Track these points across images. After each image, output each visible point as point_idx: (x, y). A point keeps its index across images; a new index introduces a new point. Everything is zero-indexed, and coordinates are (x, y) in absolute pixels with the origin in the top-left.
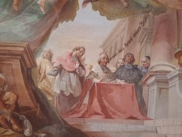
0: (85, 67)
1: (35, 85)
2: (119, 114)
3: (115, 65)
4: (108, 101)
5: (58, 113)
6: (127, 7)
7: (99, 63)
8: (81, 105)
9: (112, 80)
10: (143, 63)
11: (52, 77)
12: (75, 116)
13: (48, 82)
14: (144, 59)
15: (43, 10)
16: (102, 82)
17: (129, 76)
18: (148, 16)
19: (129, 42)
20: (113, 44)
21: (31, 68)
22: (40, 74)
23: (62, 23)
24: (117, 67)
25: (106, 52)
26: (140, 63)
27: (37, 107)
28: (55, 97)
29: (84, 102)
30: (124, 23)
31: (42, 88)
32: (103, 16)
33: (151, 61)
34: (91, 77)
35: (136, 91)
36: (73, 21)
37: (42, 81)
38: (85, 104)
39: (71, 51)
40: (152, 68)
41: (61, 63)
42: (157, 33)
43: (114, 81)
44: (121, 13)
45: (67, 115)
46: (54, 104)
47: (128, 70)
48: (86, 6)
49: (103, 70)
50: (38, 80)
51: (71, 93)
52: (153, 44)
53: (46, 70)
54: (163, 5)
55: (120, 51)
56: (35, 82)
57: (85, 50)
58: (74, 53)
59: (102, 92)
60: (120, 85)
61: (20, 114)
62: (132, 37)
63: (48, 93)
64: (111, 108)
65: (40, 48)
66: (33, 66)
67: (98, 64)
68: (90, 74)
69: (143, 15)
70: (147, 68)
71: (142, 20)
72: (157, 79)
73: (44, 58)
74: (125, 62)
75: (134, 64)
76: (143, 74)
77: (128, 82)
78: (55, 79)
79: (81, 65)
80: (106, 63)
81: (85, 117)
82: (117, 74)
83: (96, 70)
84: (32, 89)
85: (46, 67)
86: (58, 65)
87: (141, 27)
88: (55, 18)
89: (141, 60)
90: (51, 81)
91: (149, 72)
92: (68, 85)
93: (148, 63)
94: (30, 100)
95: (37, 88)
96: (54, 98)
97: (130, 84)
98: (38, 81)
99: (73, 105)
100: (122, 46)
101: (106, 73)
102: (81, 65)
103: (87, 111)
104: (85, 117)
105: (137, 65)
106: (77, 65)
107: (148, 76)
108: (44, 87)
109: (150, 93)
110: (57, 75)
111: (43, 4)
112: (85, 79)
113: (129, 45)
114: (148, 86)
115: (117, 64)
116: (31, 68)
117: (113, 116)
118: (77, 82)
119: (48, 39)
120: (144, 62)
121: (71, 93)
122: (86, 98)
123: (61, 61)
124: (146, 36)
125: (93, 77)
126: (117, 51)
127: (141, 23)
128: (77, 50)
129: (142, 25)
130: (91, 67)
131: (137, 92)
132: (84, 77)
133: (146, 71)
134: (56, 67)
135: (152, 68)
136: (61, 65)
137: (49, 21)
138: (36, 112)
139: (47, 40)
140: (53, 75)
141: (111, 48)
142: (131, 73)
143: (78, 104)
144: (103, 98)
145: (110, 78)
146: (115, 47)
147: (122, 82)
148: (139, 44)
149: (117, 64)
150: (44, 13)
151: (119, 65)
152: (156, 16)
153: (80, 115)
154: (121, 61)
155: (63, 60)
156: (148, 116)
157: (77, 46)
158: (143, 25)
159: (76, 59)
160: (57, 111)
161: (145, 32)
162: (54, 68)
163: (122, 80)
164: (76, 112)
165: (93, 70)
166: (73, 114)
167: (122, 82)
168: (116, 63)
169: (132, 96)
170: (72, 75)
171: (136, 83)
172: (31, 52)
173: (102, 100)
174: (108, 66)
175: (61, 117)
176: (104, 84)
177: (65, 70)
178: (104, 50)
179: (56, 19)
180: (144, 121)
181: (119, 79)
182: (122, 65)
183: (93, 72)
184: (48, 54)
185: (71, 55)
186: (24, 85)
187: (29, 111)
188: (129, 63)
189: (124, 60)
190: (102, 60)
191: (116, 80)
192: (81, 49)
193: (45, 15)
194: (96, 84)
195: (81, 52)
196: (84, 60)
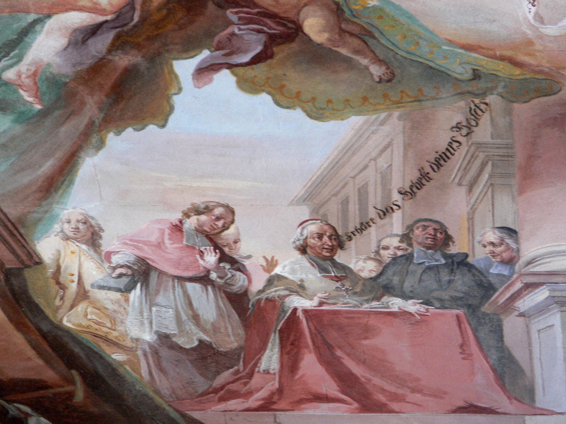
0: (246, 263)
1: (46, 318)
2: (418, 397)
3: (372, 256)
4: (362, 362)
5: (162, 397)
6: (389, 81)
7: (303, 249)
8: (250, 375)
9: (368, 301)
10: (490, 248)
11: (117, 295)
12: (233, 404)
13: (101, 309)
14: (492, 236)
15: (30, 99)
16: (324, 308)
17: (435, 286)
18: (483, 107)
19: (418, 185)
20: (351, 191)
21: (20, 270)
22: (63, 287)
23: (118, 133)
24: (379, 262)
25: (325, 215)
26: (478, 248)
27: (72, 382)
28: (140, 353)
29: (263, 365)
30: (386, 128)
31: (80, 325)
32: (288, 108)
33: (521, 241)
34: (273, 292)
35: (475, 331)
36: (163, 126)
37: (72, 307)
38: (267, 372)
39: (175, 217)
40: (529, 263)
41: (141, 254)
42: (530, 158)
43: (375, 304)
44: (365, 99)
45: (200, 402)
46: (137, 370)
47: (430, 268)
48: (211, 80)
49: (323, 270)
50: (58, 302)
51: (201, 342)
52: (521, 192)
53: (85, 277)
54: (541, 72)
55: (386, 212)
56: (48, 312)
57: (233, 212)
58: (191, 223)
59: (333, 336)
60: (404, 314)
61: (8, 401)
62: (428, 169)
63: (106, 340)
64: (377, 381)
65: (46, 212)
66: (28, 263)
67: (297, 255)
68: (270, 282)
69: (462, 103)
70: (510, 262)
71: (459, 118)
72: (557, 294)
73: (67, 238)
74: (410, 245)
75: (453, 250)
76: (492, 280)
77: (437, 304)
78: (127, 300)
79: (224, 258)
80: (332, 250)
81: (274, 407)
82: (383, 280)
83: (293, 271)
84: (39, 330)
85: (80, 266)
86: (132, 259)
87: (460, 138)
88: (86, 121)
89: (478, 238)
90: (110, 306)
91: (521, 275)
92: (184, 317)
93: (508, 248)
94: (40, 362)
95: (59, 328)
96: (136, 356)
97: (447, 311)
98: (59, 308)
99: (218, 373)
100: (387, 194)
101: (338, 279)
102: (224, 258)
103: (280, 391)
104: (274, 407)
105: (467, 256)
106: (211, 258)
107: (518, 285)
108: (85, 323)
109: (534, 335)
110: (134, 287)
111: (27, 81)
112: (253, 299)
113: (420, 194)
114: (522, 315)
115: (377, 252)
116: (20, 270)
117: (395, 406)
118: (218, 307)
119: (71, 182)
120: (492, 244)
121: (201, 342)
122: (268, 353)
123: (137, 247)
124: (489, 168)
125: (287, 292)
126: (372, 213)
127: (458, 127)
128: (198, 212)
129: (464, 131)
130: (271, 264)
131: (482, 334)
132: (245, 293)
133: (506, 273)
134: (122, 267)
135: (529, 263)
136: (142, 261)
137: (63, 129)
138: (71, 395)
139: (68, 186)
140: (119, 290)
141: (345, 202)
142: (445, 276)
143: (238, 372)
144: (339, 353)
145: (355, 293)
146: (360, 200)
147: (412, 306)
148: (463, 190)
149: (377, 252)
150: (38, 107)
151: (387, 255)
152: (515, 105)
153: (253, 402)
154: (395, 242)
155: (145, 243)
156: (538, 405)
157: (199, 201)
158: (467, 134)
159: (199, 240)
160: (157, 392)
161: (482, 156)
162: (114, 268)
163: (411, 298)
164: (234, 395)
165: (278, 270)
166: (222, 399)
167: (412, 306)
168: (374, 247)
169: (461, 346)
170: (193, 288)
171: (472, 309)
172: (9, 225)
173: (338, 359)
174: (340, 257)
175: (177, 411)
176: (336, 313)
177: (161, 273)
178: (315, 211)
179: (91, 124)
180: (527, 417)
181: (397, 296)
182: (400, 253)
183: (279, 277)
184: (81, 226)
185: (178, 228)
186: (6, 319)
187: (42, 392)
188: (429, 248)
189: (406, 238)
190: (311, 241)
191: (385, 299)
192: (218, 211)
193: (44, 114)
194: (300, 313)
195: (218, 219)
196: (236, 242)
